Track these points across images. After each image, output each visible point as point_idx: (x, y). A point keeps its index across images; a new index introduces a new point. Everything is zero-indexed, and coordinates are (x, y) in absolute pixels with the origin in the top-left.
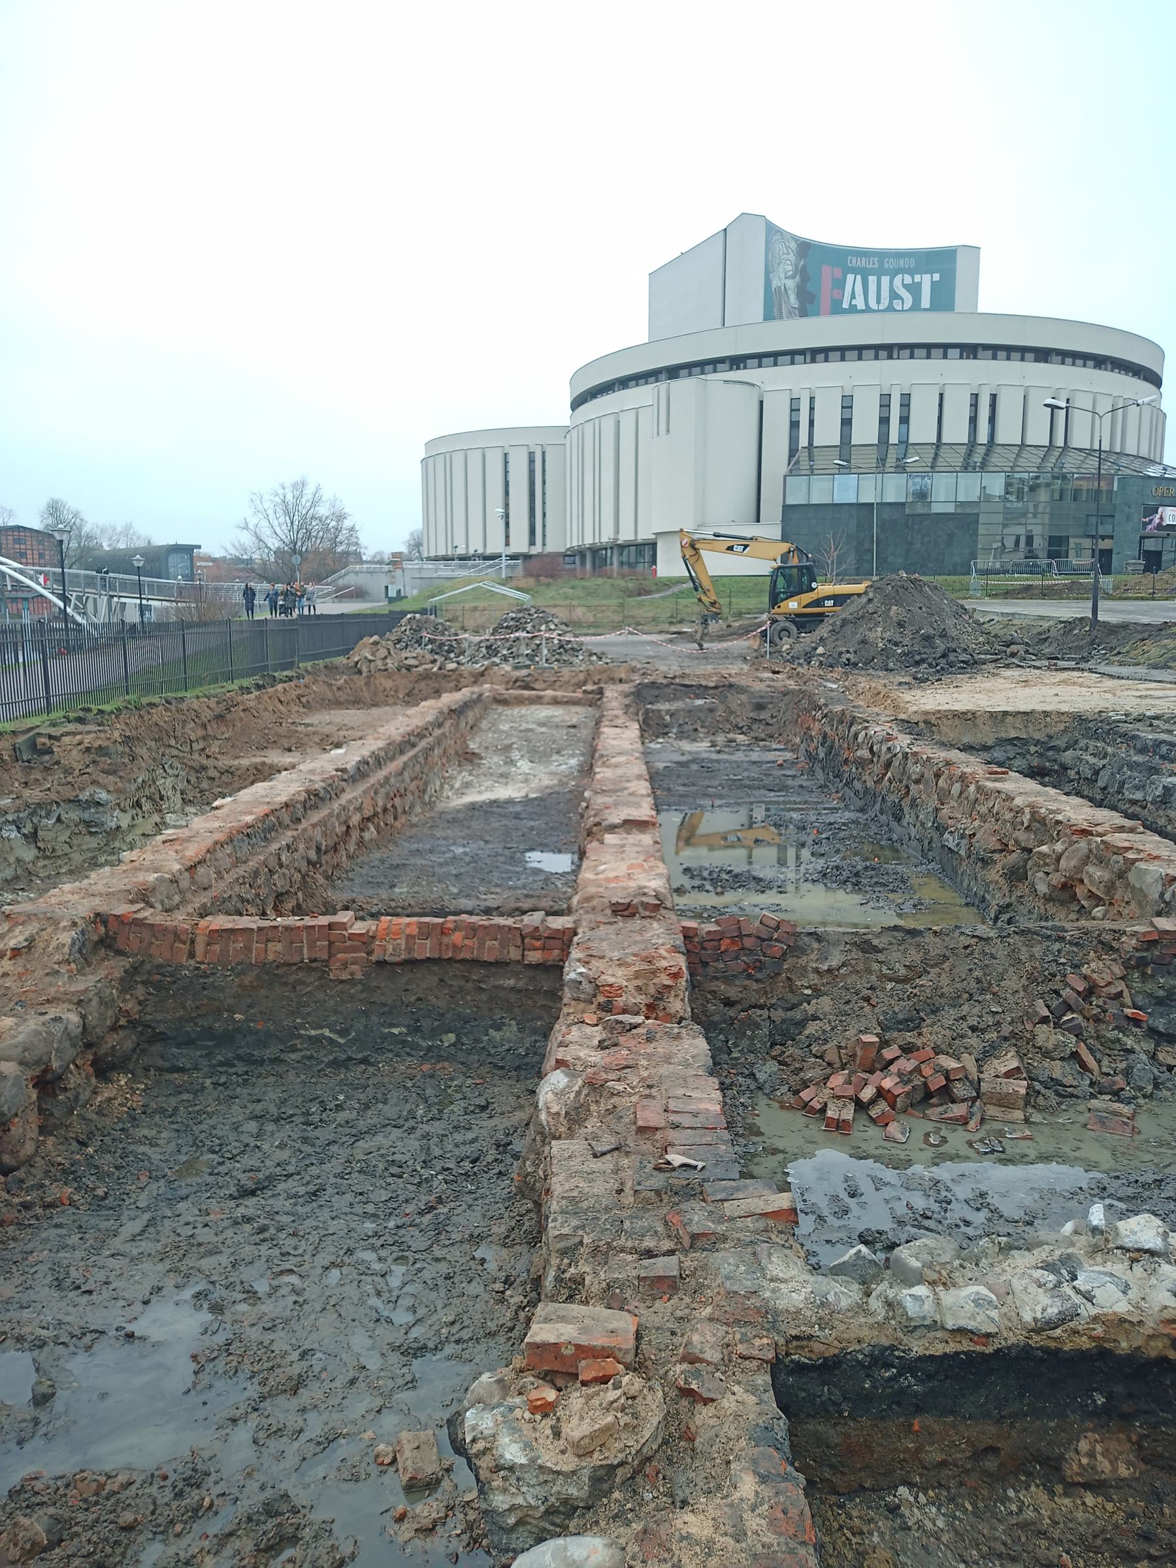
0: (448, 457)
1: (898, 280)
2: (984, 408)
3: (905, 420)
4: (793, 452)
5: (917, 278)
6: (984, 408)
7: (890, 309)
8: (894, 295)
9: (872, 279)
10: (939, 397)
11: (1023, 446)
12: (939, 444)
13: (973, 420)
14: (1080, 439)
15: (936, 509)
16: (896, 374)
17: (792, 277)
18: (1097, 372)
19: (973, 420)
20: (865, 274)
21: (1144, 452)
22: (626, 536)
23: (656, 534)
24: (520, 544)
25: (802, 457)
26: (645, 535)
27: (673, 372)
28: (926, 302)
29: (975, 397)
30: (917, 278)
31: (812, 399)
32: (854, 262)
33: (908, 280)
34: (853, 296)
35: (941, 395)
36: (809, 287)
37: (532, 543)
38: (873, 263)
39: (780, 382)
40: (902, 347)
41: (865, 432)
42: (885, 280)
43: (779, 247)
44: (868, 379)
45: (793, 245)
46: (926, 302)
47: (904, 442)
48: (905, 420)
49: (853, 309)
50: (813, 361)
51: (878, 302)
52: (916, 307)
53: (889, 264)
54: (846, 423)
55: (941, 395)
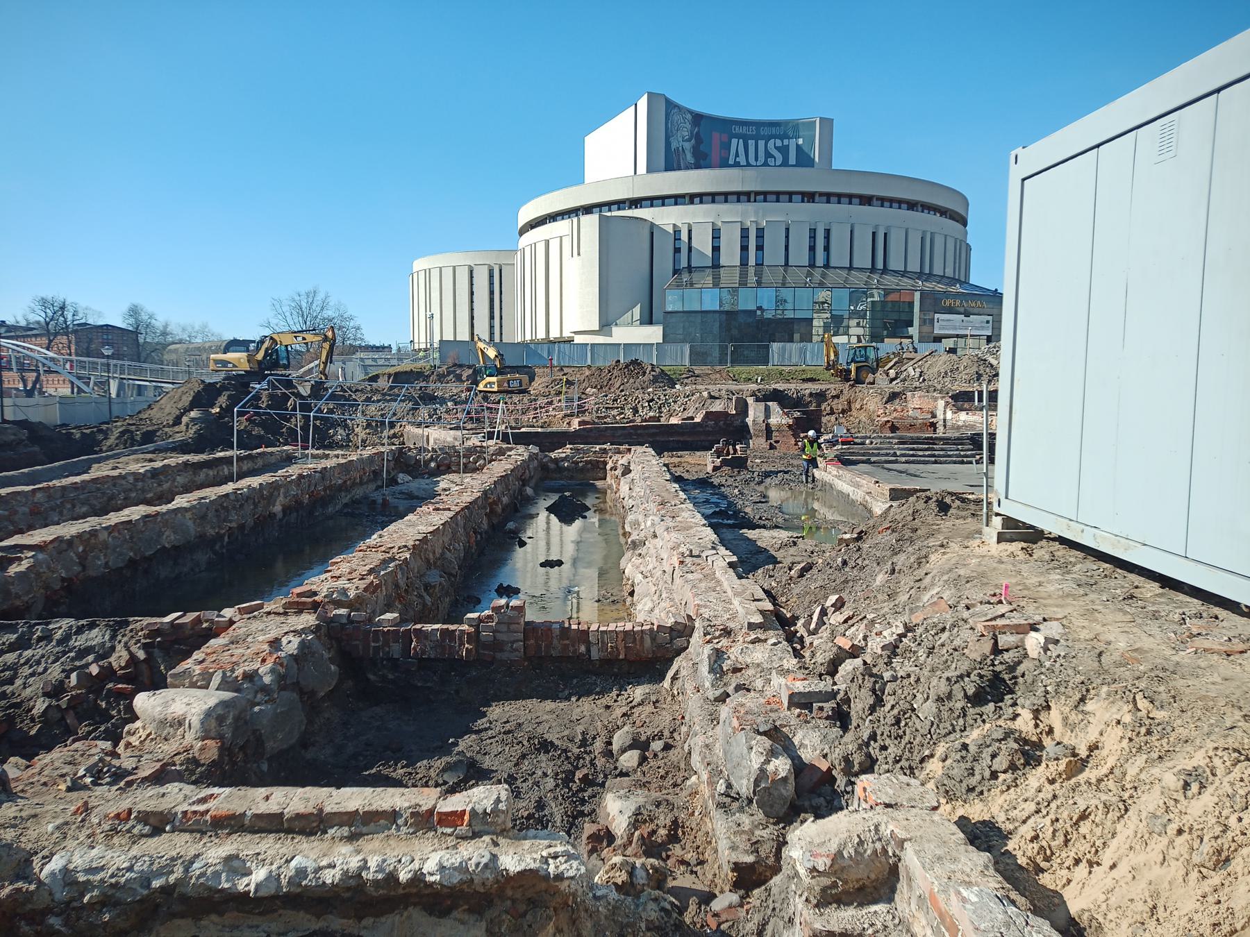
7: (766, 164)
8: (768, 155)
9: (751, 143)
11: (851, 268)
13: (812, 249)
14: (896, 264)
17: (689, 140)
18: (910, 212)
19: (812, 249)
20: (746, 139)
22: (554, 334)
23: (575, 333)
28: (792, 160)
30: (786, 142)
31: (690, 231)
32: (738, 130)
33: (779, 143)
34: (737, 155)
35: (787, 230)
36: (702, 148)
38: (752, 131)
40: (757, 193)
41: (730, 256)
42: (761, 143)
43: (677, 118)
45: (689, 116)
46: (792, 160)
48: (760, 248)
49: (737, 165)
50: (692, 203)
51: (756, 159)
52: (785, 164)
53: (765, 131)
54: (716, 249)
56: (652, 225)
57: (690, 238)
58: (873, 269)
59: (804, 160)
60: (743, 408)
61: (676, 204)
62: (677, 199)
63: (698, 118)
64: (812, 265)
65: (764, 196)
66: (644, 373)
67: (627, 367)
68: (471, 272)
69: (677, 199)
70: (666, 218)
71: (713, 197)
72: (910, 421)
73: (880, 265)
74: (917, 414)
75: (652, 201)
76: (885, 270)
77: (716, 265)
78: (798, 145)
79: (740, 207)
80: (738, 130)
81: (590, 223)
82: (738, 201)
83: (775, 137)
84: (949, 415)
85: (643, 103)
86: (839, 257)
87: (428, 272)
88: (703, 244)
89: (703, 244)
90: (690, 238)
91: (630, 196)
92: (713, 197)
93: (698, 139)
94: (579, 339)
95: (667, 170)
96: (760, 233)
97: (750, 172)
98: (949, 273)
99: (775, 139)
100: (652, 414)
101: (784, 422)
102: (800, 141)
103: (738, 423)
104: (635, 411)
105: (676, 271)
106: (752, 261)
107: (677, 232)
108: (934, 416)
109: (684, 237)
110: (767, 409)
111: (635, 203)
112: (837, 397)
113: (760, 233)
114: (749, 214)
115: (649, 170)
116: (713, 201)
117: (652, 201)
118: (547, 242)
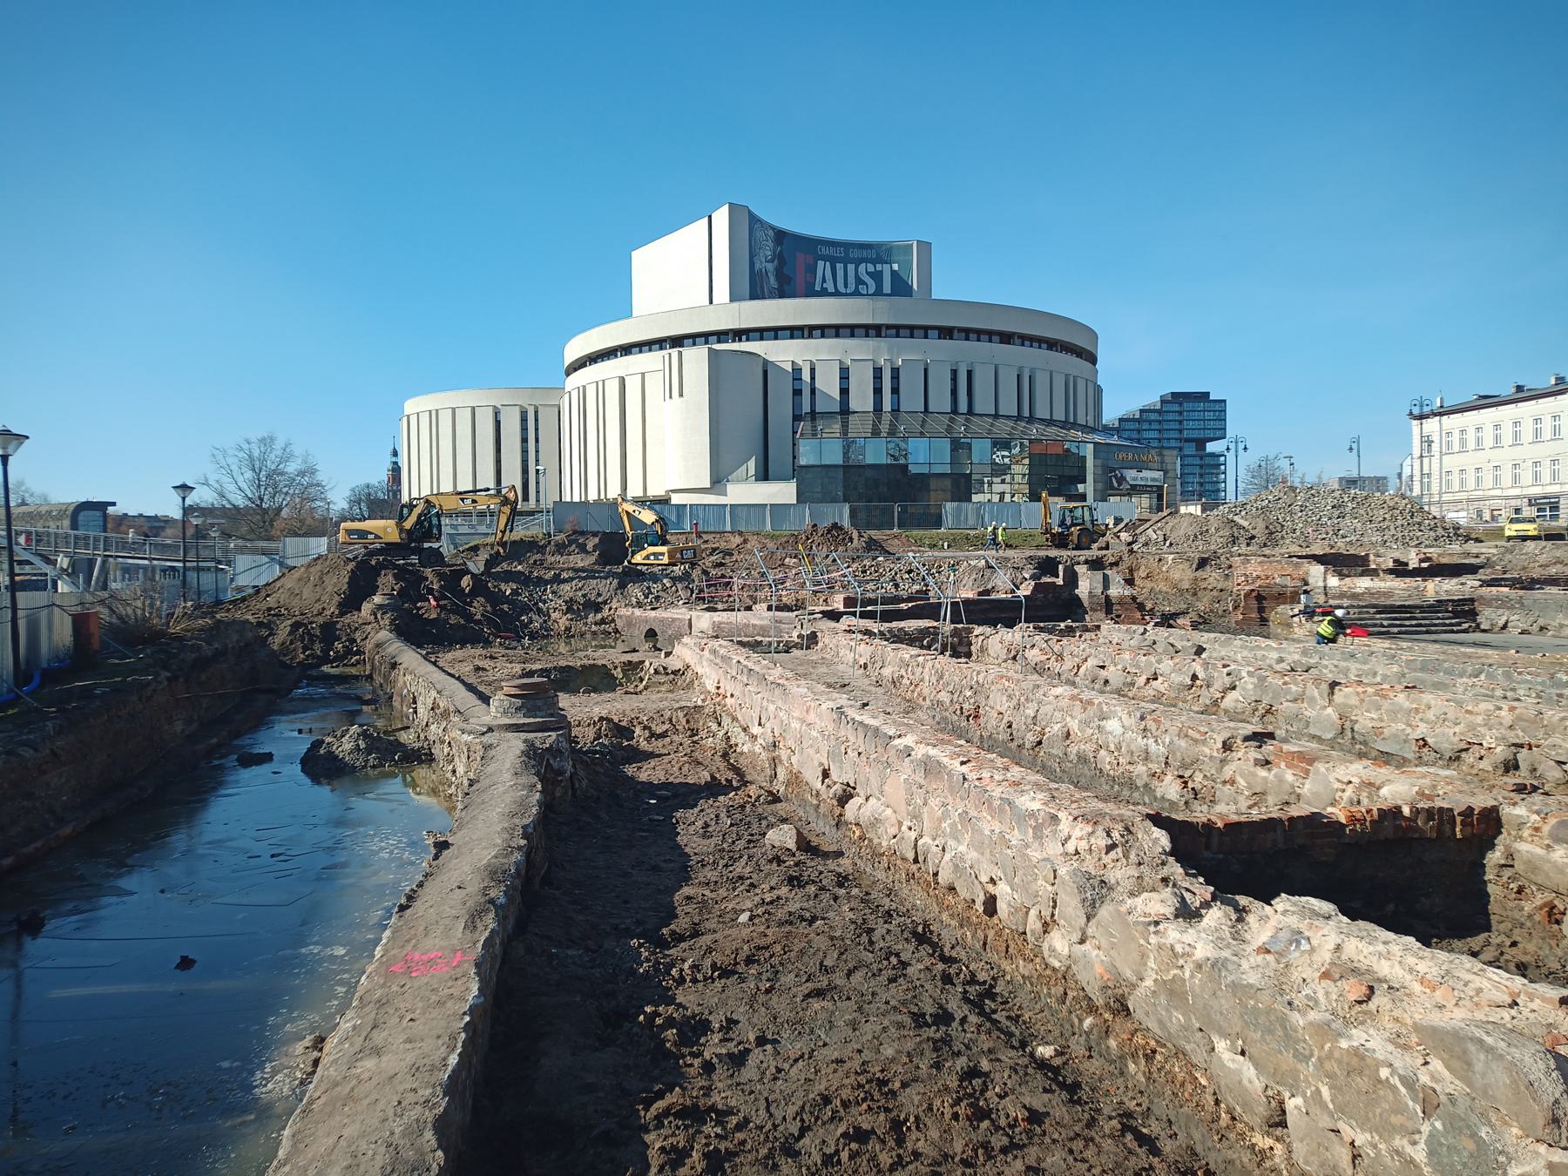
1: (862, 267)
5: (879, 267)
7: (856, 293)
8: (859, 281)
9: (839, 266)
11: (996, 416)
13: (954, 392)
14: (1042, 412)
15: (913, 469)
17: (772, 261)
19: (954, 392)
28: (887, 288)
29: (954, 373)
30: (879, 267)
31: (813, 370)
32: (825, 251)
33: (871, 268)
34: (824, 280)
36: (786, 271)
38: (839, 252)
40: (889, 327)
41: (861, 400)
42: (851, 267)
43: (759, 234)
45: (771, 233)
46: (887, 288)
48: (895, 390)
49: (824, 293)
52: (879, 292)
53: (855, 254)
54: (844, 391)
56: (766, 362)
57: (813, 378)
58: (1019, 417)
59: (901, 287)
60: (1072, 578)
61: (792, 337)
62: (795, 332)
63: (781, 236)
64: (955, 411)
65: (897, 330)
66: (851, 540)
67: (829, 531)
68: (497, 413)
69: (795, 332)
70: (783, 353)
71: (836, 331)
72: (1278, 589)
73: (1026, 414)
74: (1288, 582)
75: (761, 333)
76: (1032, 419)
77: (845, 411)
78: (893, 273)
79: (871, 343)
80: (825, 251)
81: (696, 358)
82: (867, 336)
83: (866, 261)
84: (1333, 581)
85: (721, 217)
86: (983, 404)
87: (434, 415)
88: (829, 385)
89: (829, 385)
90: (813, 378)
91: (736, 326)
92: (836, 331)
93: (780, 259)
94: (676, 499)
95: (753, 297)
97: (882, 303)
98: (1059, 415)
99: (869, 265)
100: (916, 587)
101: (1127, 593)
102: (895, 267)
103: (1065, 595)
104: (897, 586)
105: (797, 418)
106: (887, 406)
107: (797, 371)
108: (1306, 584)
109: (806, 376)
110: (1106, 578)
111: (739, 334)
112: (1116, 564)
113: (896, 372)
114: (880, 351)
115: (734, 298)
116: (837, 336)
117: (761, 333)
118: (622, 381)
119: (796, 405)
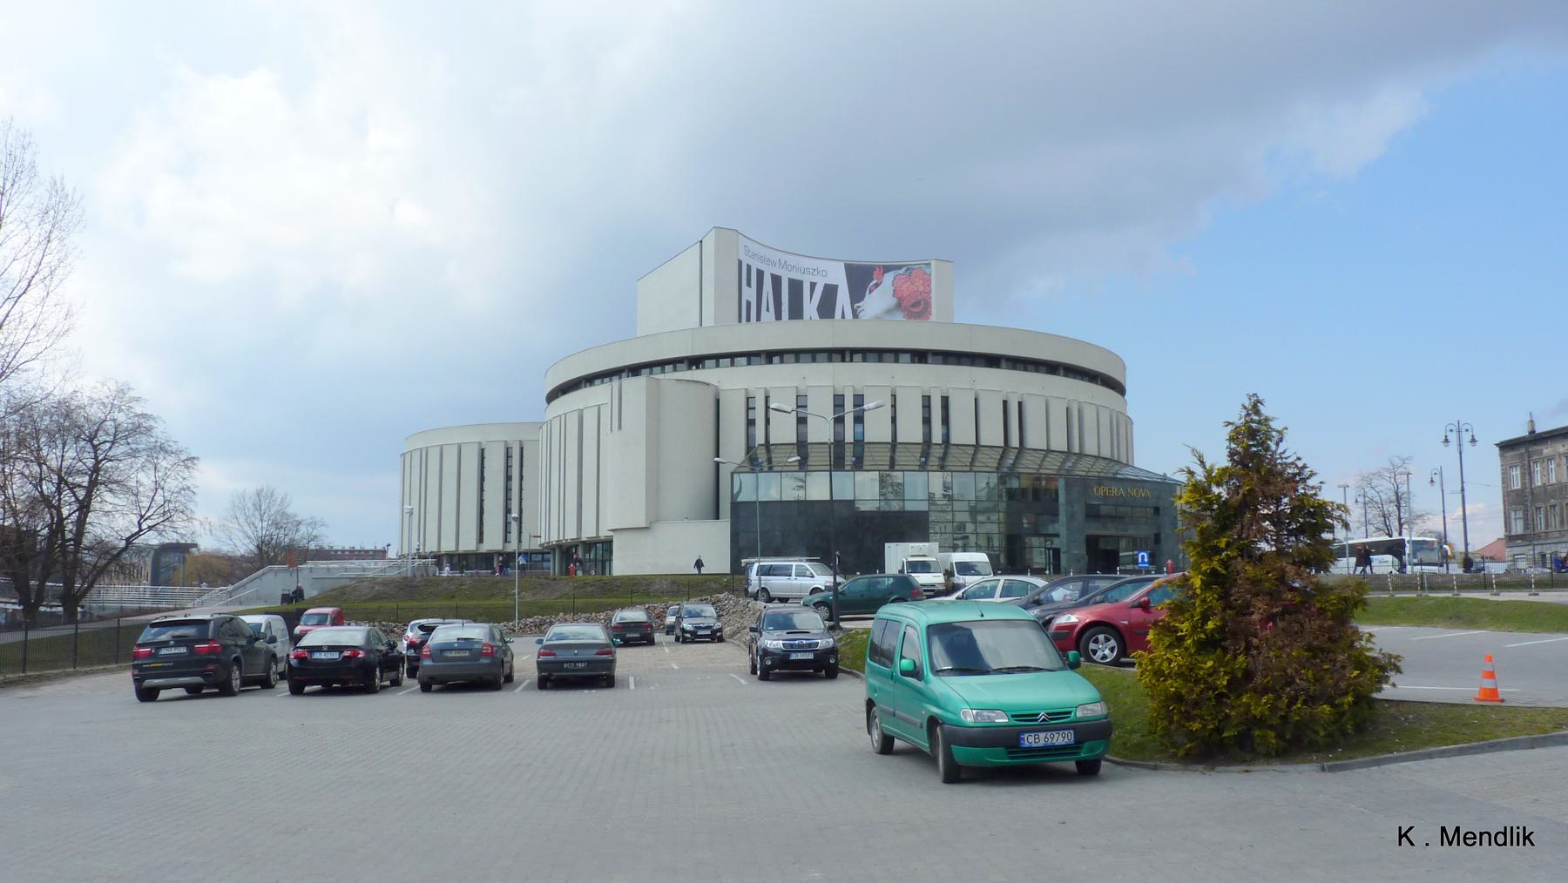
0: (424, 453)
2: (936, 410)
3: (859, 419)
4: (750, 448)
6: (936, 410)
10: (893, 399)
11: (977, 446)
12: (894, 444)
13: (927, 421)
14: (1035, 440)
16: (851, 376)
19: (927, 421)
21: (1106, 453)
22: (588, 533)
24: (493, 542)
25: (759, 458)
26: (604, 534)
27: (635, 370)
37: (506, 540)
39: (734, 381)
44: (822, 380)
47: (859, 443)
48: (859, 419)
50: (770, 362)
54: (802, 421)
55: (894, 396)
96: (859, 400)
119: (749, 437)
